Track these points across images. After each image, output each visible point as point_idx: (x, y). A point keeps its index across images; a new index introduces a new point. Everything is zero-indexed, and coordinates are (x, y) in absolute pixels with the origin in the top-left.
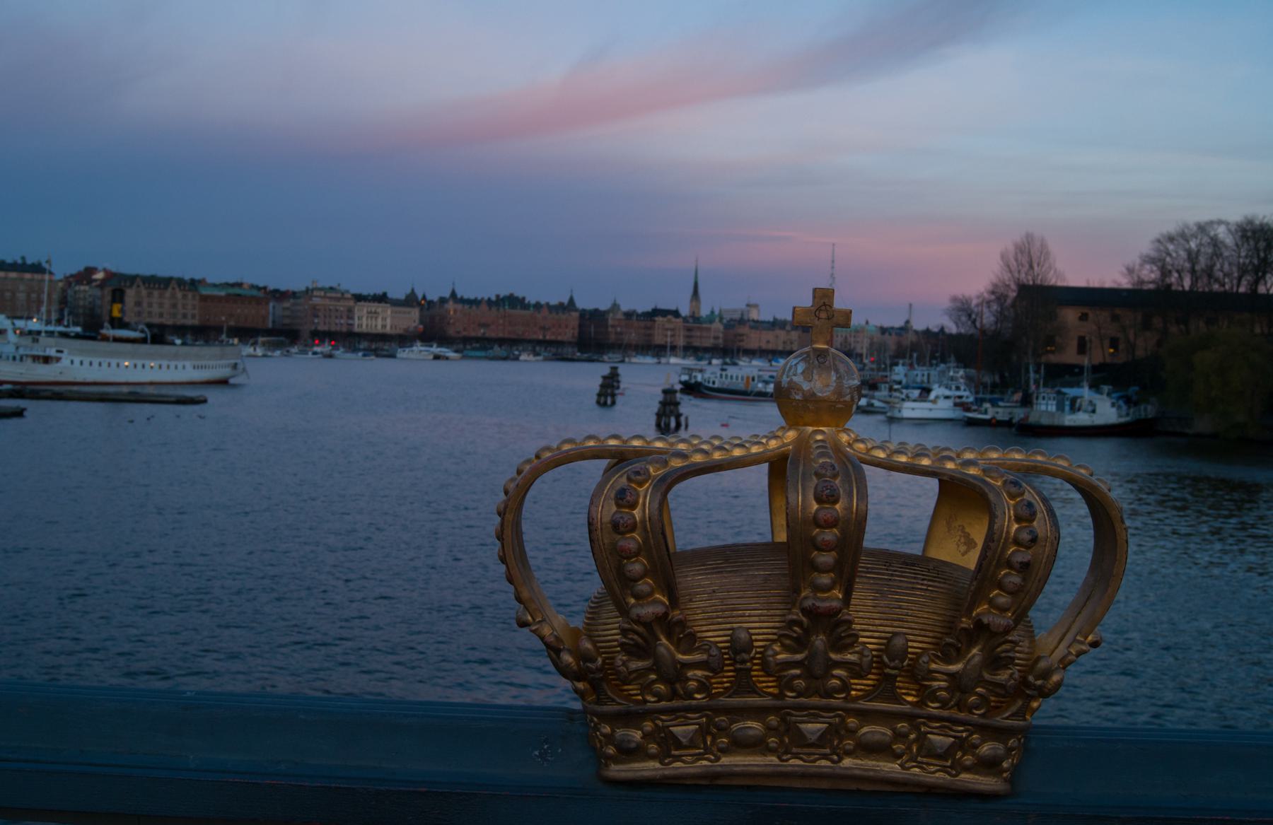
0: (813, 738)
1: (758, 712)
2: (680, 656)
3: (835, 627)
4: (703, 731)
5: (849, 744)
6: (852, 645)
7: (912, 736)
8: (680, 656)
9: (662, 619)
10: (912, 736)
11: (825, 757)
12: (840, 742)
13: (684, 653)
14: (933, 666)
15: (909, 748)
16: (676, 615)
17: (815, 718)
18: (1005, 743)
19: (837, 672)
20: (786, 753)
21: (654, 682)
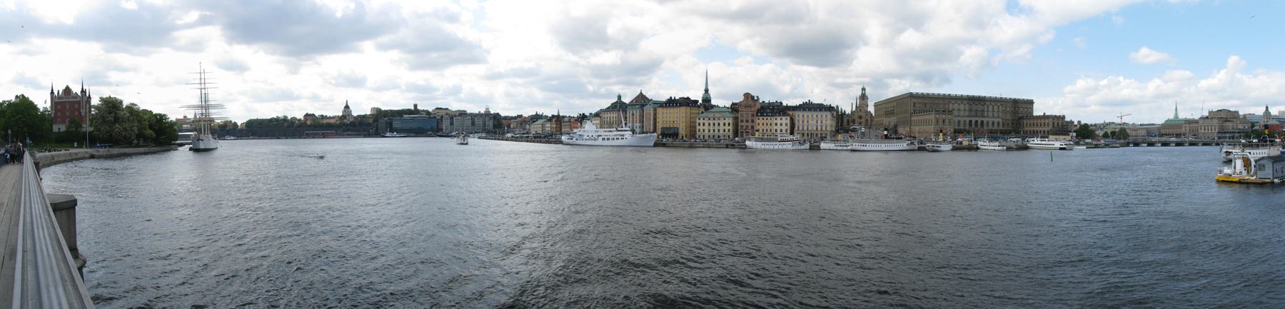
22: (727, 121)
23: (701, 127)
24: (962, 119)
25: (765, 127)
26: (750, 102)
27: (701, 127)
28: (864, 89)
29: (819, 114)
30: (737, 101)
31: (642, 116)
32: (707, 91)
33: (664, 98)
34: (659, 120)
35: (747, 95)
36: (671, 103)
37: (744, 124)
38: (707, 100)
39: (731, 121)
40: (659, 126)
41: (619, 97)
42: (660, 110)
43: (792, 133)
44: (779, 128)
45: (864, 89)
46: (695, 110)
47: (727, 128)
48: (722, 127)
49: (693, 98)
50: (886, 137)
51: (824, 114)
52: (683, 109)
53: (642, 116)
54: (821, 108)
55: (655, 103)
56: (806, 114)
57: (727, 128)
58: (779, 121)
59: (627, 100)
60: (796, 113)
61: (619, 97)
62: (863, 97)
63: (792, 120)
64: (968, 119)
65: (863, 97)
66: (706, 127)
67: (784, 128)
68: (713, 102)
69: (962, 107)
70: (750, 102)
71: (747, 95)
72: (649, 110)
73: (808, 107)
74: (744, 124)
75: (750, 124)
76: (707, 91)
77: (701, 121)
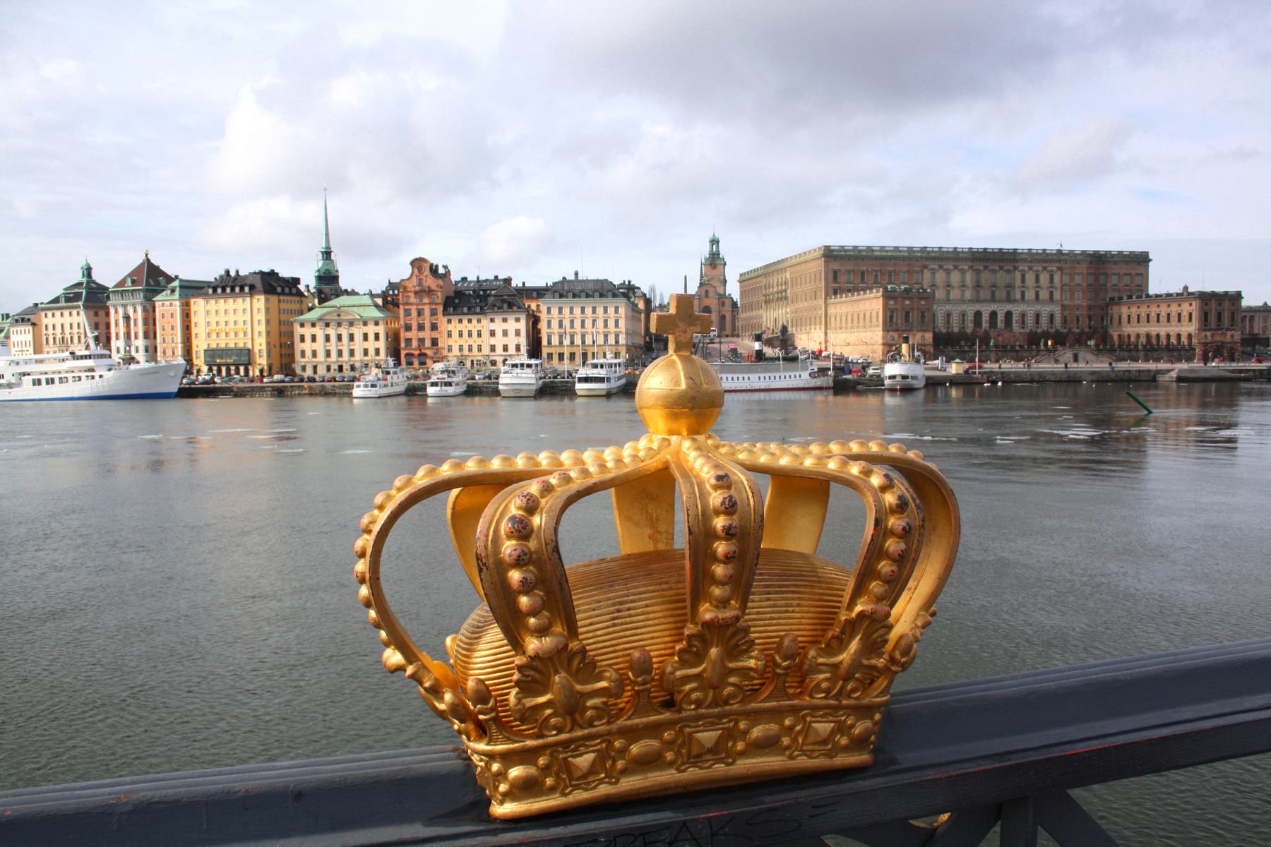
0: (709, 745)
1: (654, 730)
2: (578, 687)
3: (732, 636)
4: (602, 756)
5: (740, 746)
6: (747, 651)
7: (798, 728)
8: (578, 687)
10: (798, 728)
11: (719, 761)
12: (734, 745)
13: (583, 683)
14: (821, 660)
15: (795, 740)
16: (574, 645)
17: (710, 726)
18: (872, 718)
19: (732, 680)
20: (684, 763)
21: (550, 716)
23: (308, 346)
24: (956, 310)
25: (466, 341)
26: (430, 282)
27: (308, 346)
28: (714, 242)
29: (600, 305)
30: (395, 280)
31: (150, 321)
32: (327, 254)
33: (209, 273)
34: (199, 330)
35: (417, 263)
36: (230, 285)
37: (414, 334)
39: (381, 329)
40: (200, 345)
41: (88, 271)
42: (199, 306)
43: (38, 350)
44: (499, 341)
45: (714, 242)
46: (290, 303)
47: (371, 345)
48: (358, 345)
49: (285, 273)
50: (760, 356)
51: (611, 304)
52: (260, 301)
53: (150, 321)
54: (602, 290)
56: (566, 304)
57: (371, 345)
58: (498, 326)
59: (107, 277)
61: (88, 271)
62: (714, 261)
63: (534, 321)
64: (971, 310)
65: (714, 261)
66: (320, 346)
67: (512, 341)
68: (344, 284)
69: (955, 277)
70: (430, 282)
71: (417, 263)
72: (168, 305)
73: (566, 290)
74: (414, 334)
75: (427, 335)
76: (327, 254)
77: (308, 331)
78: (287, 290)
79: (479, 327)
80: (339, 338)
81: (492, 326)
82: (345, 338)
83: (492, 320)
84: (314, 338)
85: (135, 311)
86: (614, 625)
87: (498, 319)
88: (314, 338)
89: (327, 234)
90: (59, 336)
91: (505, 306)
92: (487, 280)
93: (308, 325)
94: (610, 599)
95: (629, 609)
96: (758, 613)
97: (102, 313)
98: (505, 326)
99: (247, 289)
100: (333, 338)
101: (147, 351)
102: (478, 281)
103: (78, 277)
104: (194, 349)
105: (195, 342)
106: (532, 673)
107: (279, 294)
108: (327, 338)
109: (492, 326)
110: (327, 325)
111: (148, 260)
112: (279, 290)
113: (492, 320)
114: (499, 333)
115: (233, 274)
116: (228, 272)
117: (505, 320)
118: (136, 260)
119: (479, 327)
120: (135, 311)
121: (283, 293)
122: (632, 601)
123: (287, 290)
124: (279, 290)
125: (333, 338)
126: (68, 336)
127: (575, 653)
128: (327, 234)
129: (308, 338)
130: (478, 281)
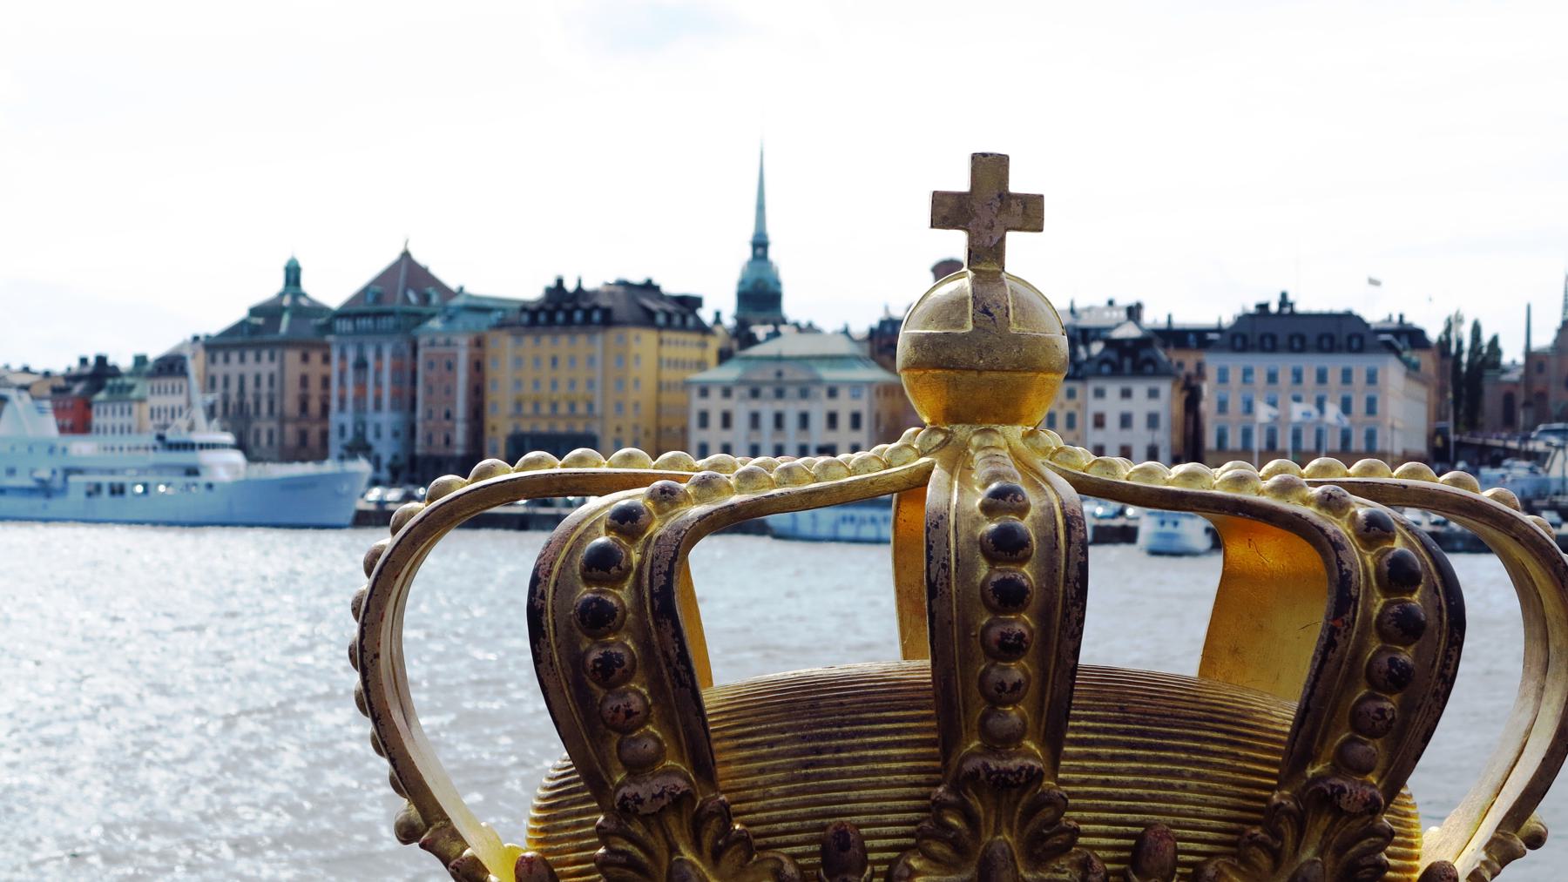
9: (679, 802)
22: (844, 406)
32: (760, 245)
38: (760, 297)
40: (500, 425)
41: (293, 274)
42: (505, 350)
46: (682, 347)
49: (672, 286)
54: (1340, 334)
55: (480, 308)
56: (1261, 363)
58: (1112, 405)
60: (1213, 363)
61: (293, 274)
68: (792, 308)
76: (760, 245)
78: (677, 320)
79: (1070, 406)
80: (779, 420)
81: (1095, 406)
82: (791, 422)
83: (1099, 394)
84: (727, 421)
85: (379, 356)
86: (807, 777)
87: (1113, 388)
88: (727, 421)
89: (761, 208)
90: (234, 399)
91: (1127, 362)
92: (1089, 309)
93: (715, 394)
94: (801, 728)
95: (839, 749)
96: (1106, 783)
97: (316, 357)
98: (1126, 406)
99: (596, 316)
100: (767, 421)
101: (396, 434)
102: (1072, 311)
103: (270, 287)
104: (488, 433)
105: (491, 419)
106: (630, 847)
107: (660, 328)
108: (755, 419)
109: (1095, 406)
110: (755, 394)
111: (406, 255)
112: (661, 319)
113: (1099, 394)
114: (1112, 421)
115: (570, 286)
116: (560, 282)
117: (1126, 394)
118: (392, 256)
119: (1070, 406)
120: (379, 356)
121: (668, 325)
122: (845, 736)
123: (677, 320)
124: (661, 319)
125: (767, 421)
126: (250, 399)
127: (712, 815)
128: (761, 208)
129: (715, 420)
130: (1072, 311)
